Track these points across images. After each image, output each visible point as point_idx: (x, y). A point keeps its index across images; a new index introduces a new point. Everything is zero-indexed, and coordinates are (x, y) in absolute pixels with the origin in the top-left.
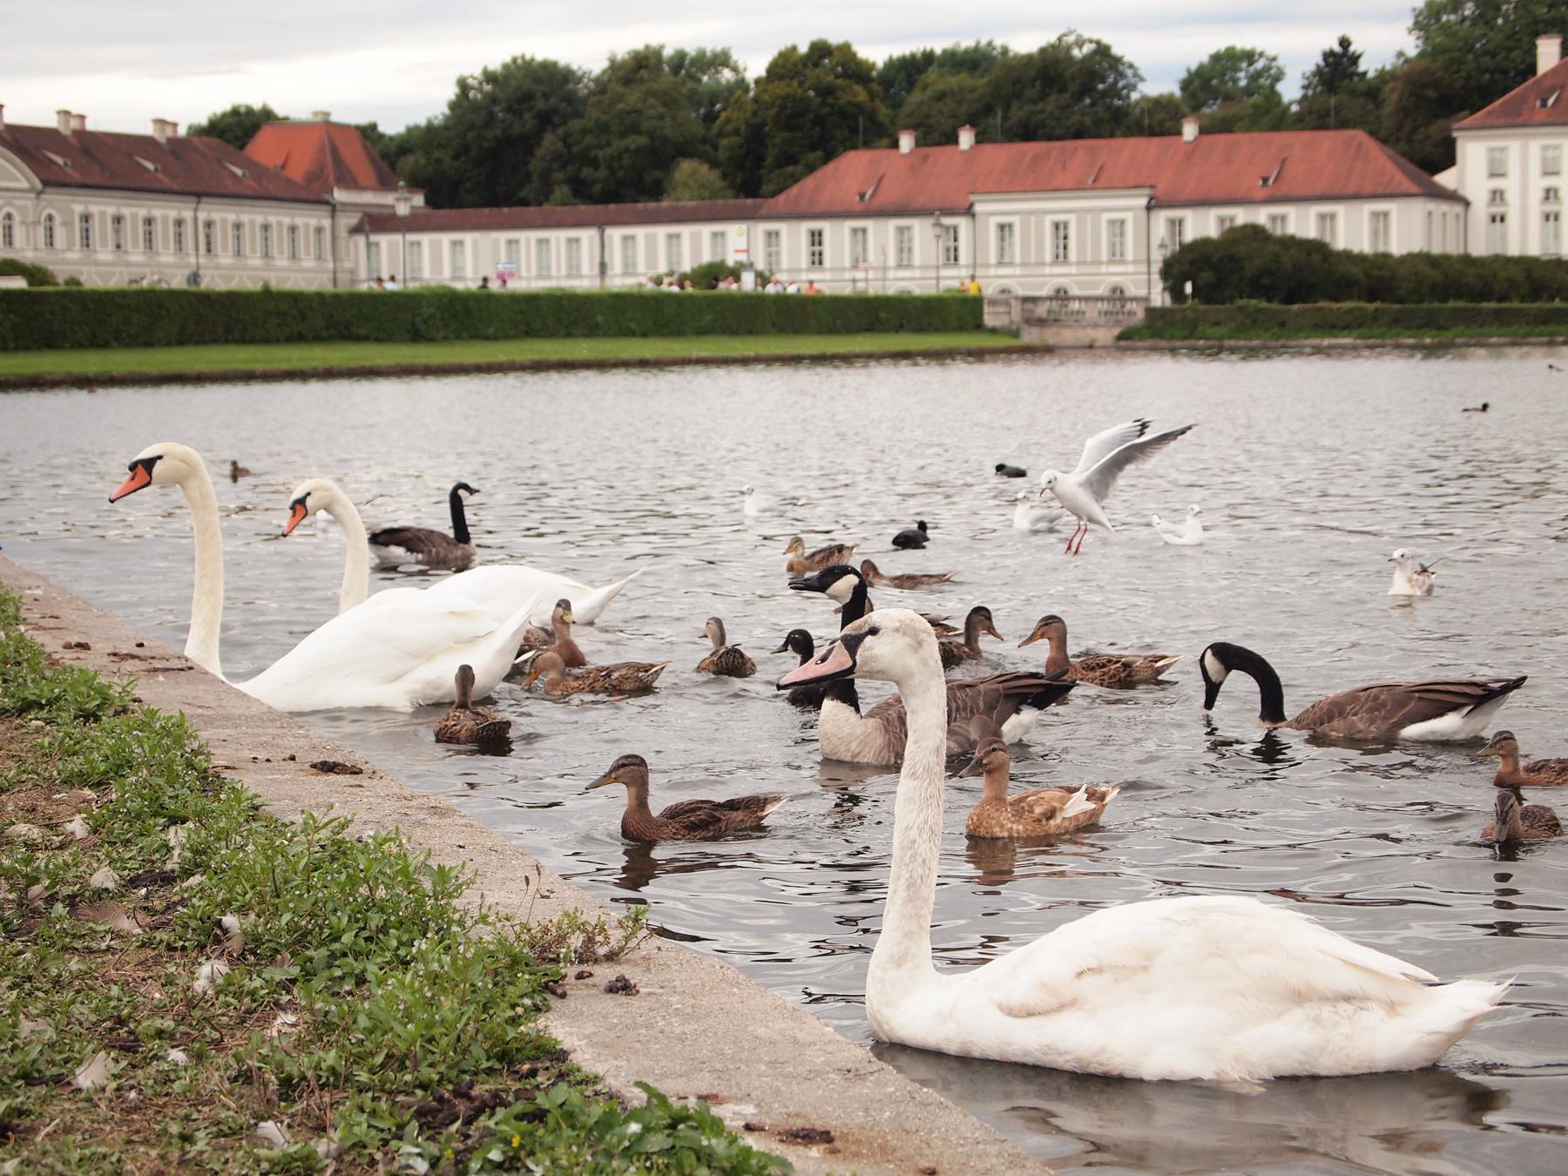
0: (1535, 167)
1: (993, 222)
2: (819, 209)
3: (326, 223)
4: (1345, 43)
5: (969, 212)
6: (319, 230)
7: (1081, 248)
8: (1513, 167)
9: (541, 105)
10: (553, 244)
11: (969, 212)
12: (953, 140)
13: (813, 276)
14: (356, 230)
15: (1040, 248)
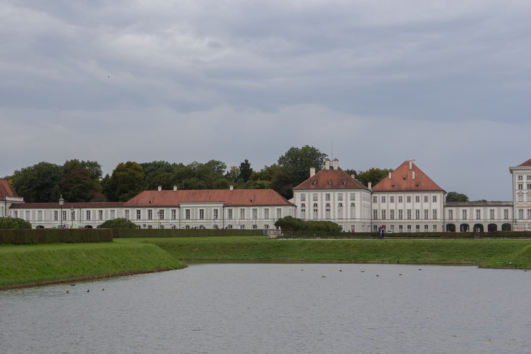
0: (312, 199)
1: (185, 209)
2: (139, 205)
3: (4, 206)
4: (246, 161)
5: (179, 207)
6: (3, 207)
7: (207, 216)
8: (307, 199)
9: (53, 175)
10: (58, 212)
11: (179, 207)
12: (173, 189)
13: (161, 221)
14: (11, 207)
15: (197, 216)
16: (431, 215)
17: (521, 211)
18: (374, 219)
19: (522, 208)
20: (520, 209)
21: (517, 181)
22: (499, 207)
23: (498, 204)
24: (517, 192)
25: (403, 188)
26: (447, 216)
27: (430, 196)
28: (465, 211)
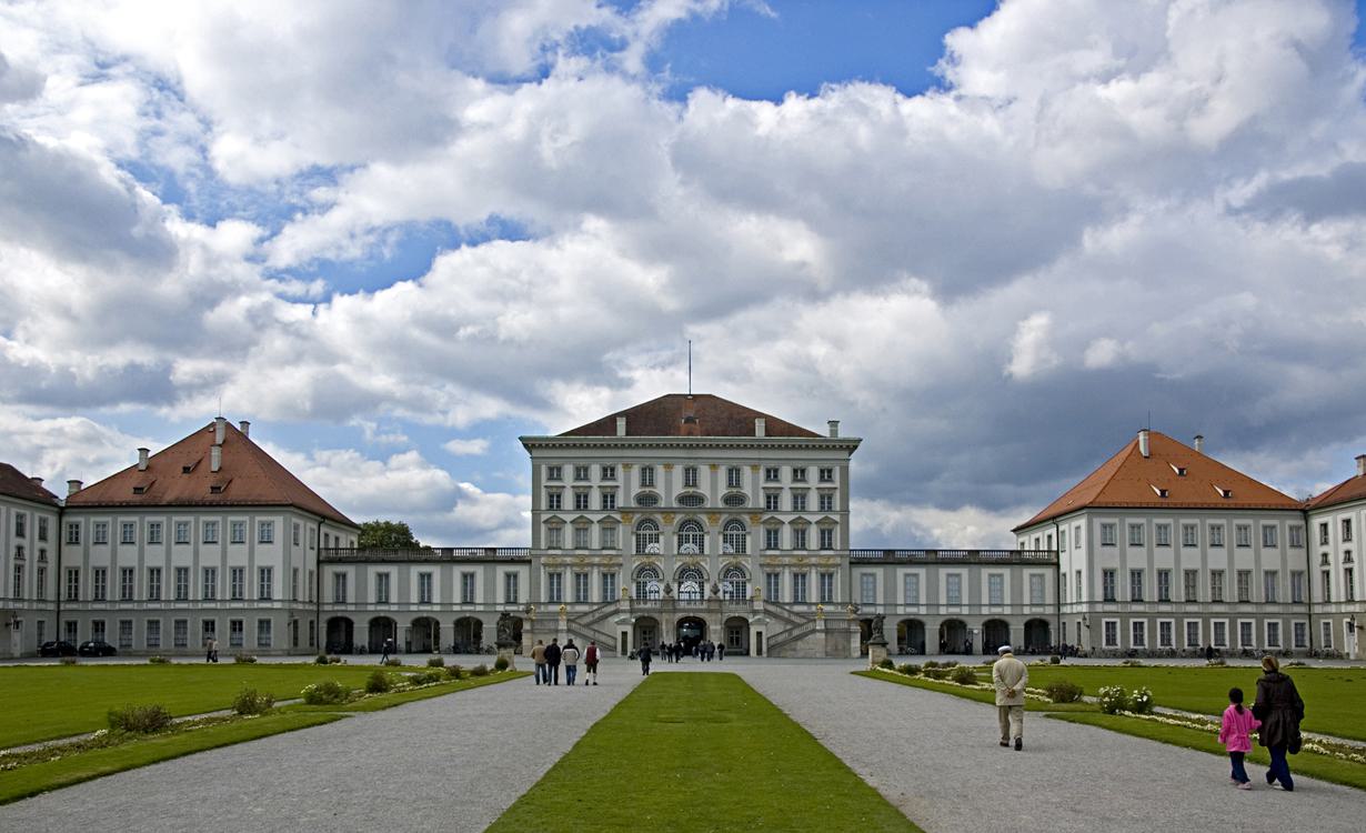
16: (251, 589)
17: (555, 578)
18: (69, 600)
19: (559, 570)
20: (551, 570)
21: (544, 482)
22: (490, 567)
23: (491, 558)
24: (544, 517)
25: (169, 497)
26: (328, 594)
27: (251, 522)
28: (425, 578)
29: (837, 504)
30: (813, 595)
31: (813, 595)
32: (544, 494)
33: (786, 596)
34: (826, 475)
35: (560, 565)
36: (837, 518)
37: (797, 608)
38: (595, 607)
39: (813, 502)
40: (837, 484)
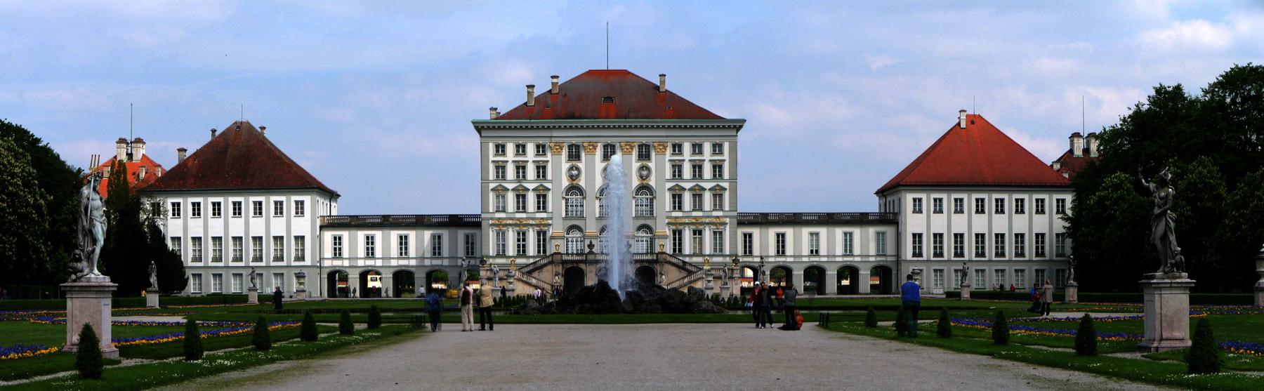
21: (492, 158)
24: (492, 186)
29: (726, 175)
30: (708, 249)
31: (708, 249)
32: (492, 167)
33: (687, 249)
34: (717, 148)
35: (506, 225)
36: (726, 185)
37: (695, 259)
38: (532, 261)
39: (707, 171)
40: (726, 156)
